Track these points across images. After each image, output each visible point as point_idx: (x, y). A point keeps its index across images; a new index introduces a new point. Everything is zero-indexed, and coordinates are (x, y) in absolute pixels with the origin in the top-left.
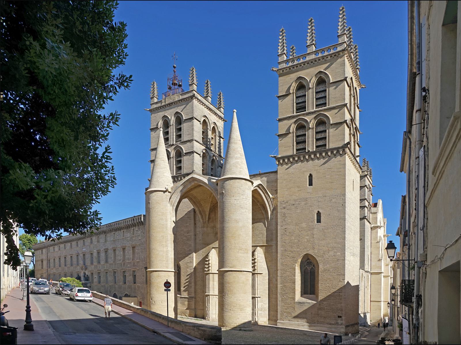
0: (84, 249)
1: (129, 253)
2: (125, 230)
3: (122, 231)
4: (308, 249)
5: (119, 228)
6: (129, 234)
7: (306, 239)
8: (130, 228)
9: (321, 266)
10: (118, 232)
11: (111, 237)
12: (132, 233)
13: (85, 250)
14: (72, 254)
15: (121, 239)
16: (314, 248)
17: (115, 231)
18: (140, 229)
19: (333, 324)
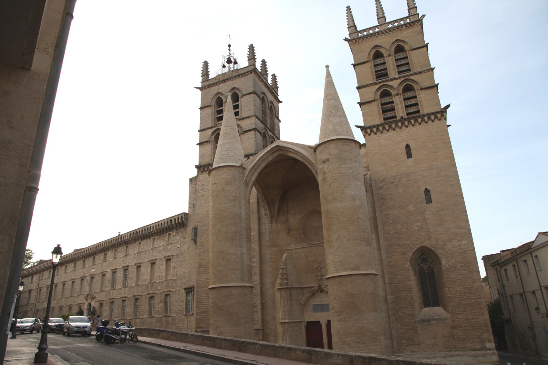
0: (92, 270)
1: (160, 268)
2: (156, 237)
3: (152, 239)
4: (423, 240)
5: (147, 234)
6: (162, 241)
7: (417, 226)
8: (163, 233)
9: (444, 262)
10: (145, 240)
11: (135, 248)
12: (167, 239)
13: (95, 271)
14: (75, 279)
15: (150, 250)
16: (429, 238)
17: (141, 240)
18: (178, 233)
19: (479, 350)
